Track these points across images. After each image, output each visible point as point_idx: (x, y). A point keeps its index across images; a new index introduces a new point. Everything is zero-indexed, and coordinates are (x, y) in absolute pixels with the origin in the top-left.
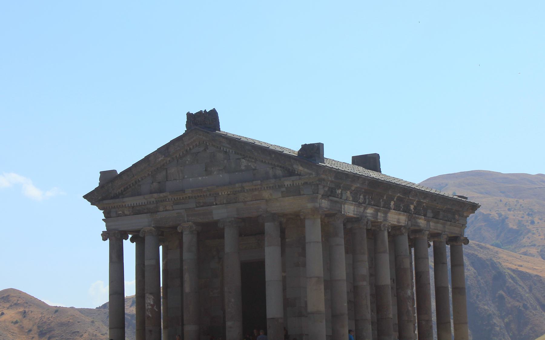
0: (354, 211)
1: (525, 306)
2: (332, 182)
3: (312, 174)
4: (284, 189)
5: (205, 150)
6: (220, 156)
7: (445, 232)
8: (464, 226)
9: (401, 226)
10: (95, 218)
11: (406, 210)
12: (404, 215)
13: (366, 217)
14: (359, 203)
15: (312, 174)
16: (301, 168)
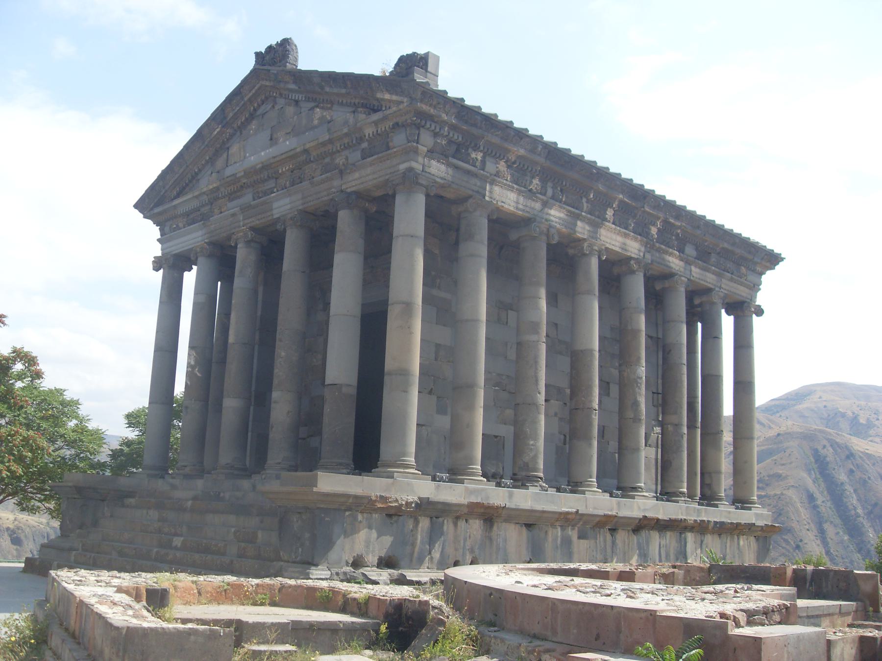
0: (517, 203)
1: (869, 478)
2: (453, 127)
3: (403, 102)
4: (365, 145)
5: (273, 107)
6: (290, 110)
7: (720, 288)
8: (755, 287)
9: (631, 258)
10: (147, 238)
11: (641, 231)
12: (636, 240)
13: (547, 220)
14: (530, 190)
15: (403, 102)
16: (387, 96)
